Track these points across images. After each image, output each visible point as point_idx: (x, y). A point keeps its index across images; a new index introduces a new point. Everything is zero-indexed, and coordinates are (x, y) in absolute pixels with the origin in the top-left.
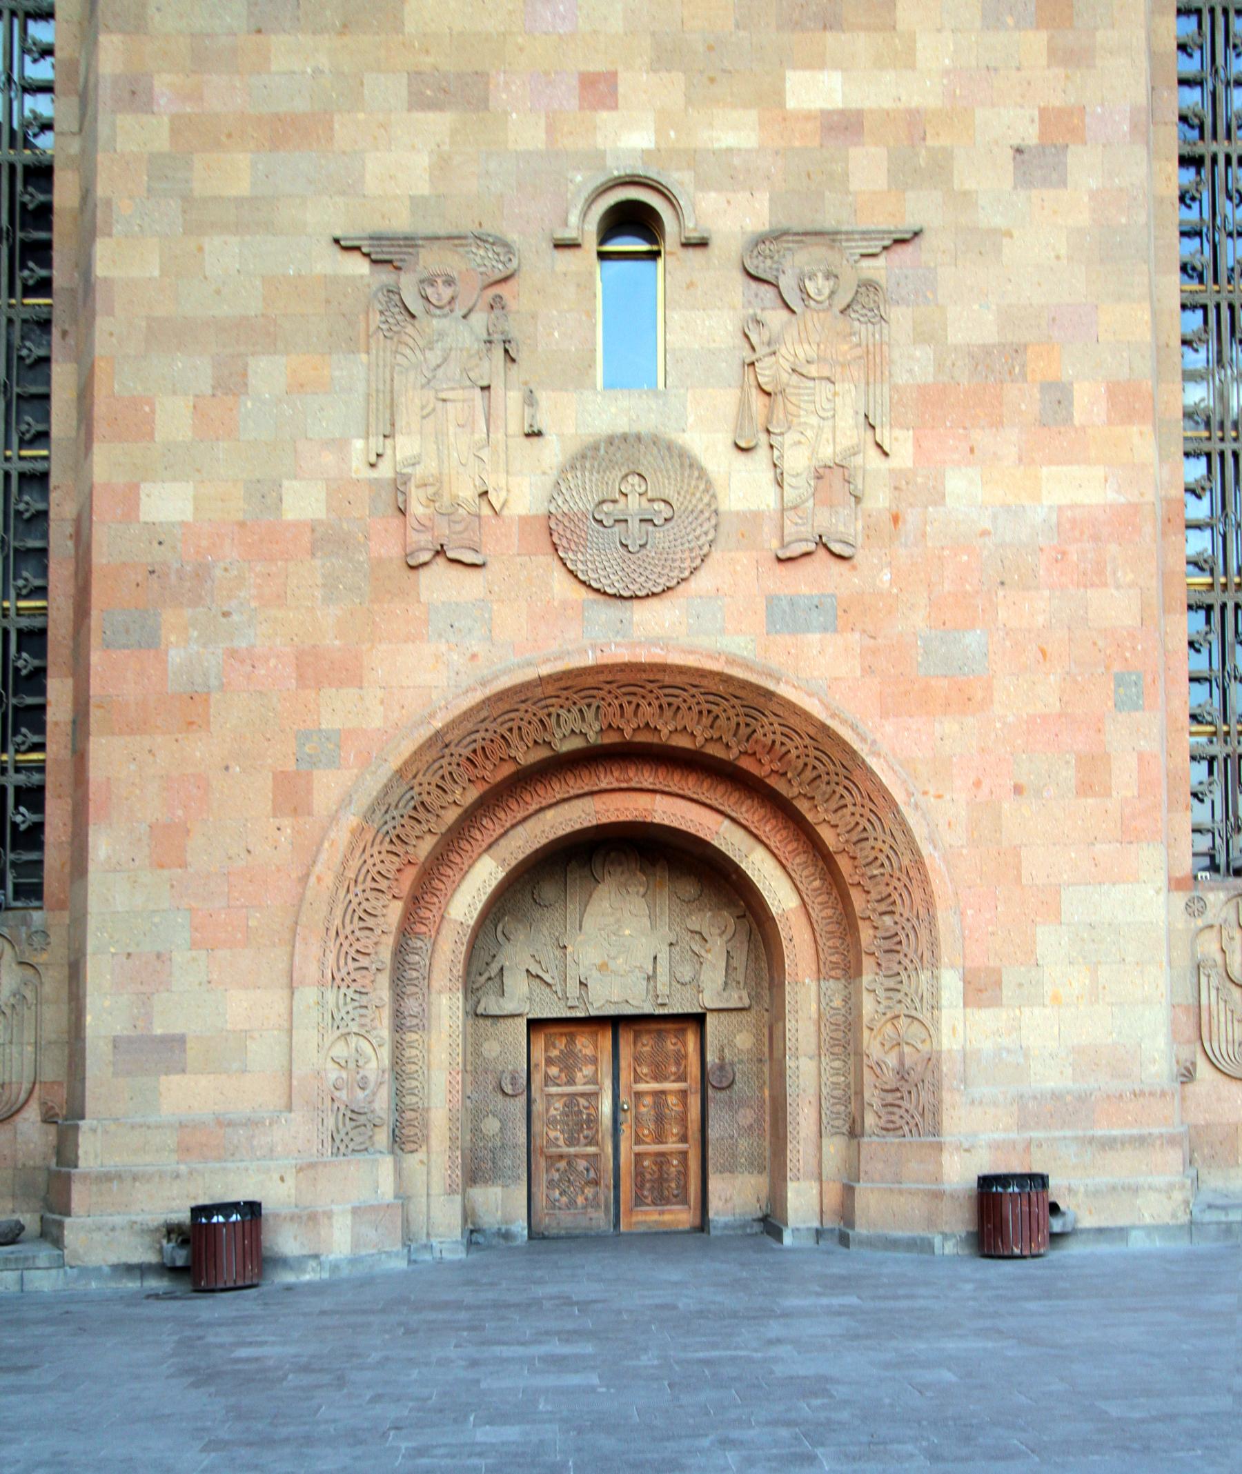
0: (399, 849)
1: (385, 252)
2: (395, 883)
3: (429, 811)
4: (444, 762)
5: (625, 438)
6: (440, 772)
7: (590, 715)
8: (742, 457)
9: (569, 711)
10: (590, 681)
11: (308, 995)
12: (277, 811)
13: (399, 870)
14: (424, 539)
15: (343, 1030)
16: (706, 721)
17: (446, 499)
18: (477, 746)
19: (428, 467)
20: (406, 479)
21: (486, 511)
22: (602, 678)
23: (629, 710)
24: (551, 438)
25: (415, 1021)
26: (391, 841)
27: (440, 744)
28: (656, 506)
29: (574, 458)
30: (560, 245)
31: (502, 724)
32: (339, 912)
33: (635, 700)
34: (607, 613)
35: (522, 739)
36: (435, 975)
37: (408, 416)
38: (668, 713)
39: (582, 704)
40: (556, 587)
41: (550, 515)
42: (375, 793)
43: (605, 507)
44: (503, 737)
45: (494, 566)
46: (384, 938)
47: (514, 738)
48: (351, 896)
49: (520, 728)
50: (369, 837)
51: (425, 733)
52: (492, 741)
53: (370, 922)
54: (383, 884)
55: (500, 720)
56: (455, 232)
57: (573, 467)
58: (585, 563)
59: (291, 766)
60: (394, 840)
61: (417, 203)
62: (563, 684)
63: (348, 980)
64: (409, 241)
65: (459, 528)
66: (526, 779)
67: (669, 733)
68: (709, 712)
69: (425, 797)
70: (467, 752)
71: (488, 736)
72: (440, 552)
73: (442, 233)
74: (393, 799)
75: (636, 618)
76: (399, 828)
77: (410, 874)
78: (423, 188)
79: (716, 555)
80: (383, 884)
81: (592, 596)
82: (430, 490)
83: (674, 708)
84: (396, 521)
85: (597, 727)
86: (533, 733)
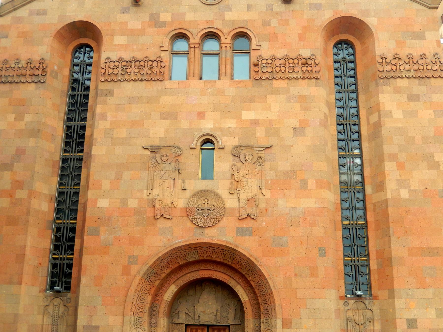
0: (151, 284)
1: (154, 149)
5: (204, 191)
7: (196, 253)
8: (231, 195)
10: (195, 246)
11: (127, 318)
12: (123, 274)
14: (159, 213)
15: (136, 327)
17: (164, 204)
19: (160, 197)
20: (155, 199)
21: (173, 206)
22: (198, 245)
23: (205, 253)
24: (188, 191)
25: (154, 325)
27: (160, 260)
28: (211, 206)
29: (193, 195)
30: (191, 148)
32: (136, 298)
33: (206, 250)
34: (199, 231)
36: (160, 313)
37: (156, 185)
38: (214, 254)
39: (194, 251)
40: (188, 224)
41: (187, 208)
43: (199, 206)
45: (174, 220)
46: (147, 305)
47: (178, 258)
48: (139, 295)
50: (143, 281)
51: (157, 257)
53: (143, 301)
54: (147, 292)
56: (169, 145)
57: (192, 197)
58: (194, 219)
59: (126, 264)
61: (161, 139)
62: (189, 247)
63: (137, 315)
64: (159, 147)
65: (167, 210)
66: (181, 267)
67: (214, 258)
69: (157, 272)
70: (167, 261)
72: (162, 216)
73: (166, 145)
74: (149, 272)
75: (206, 232)
77: (153, 290)
78: (162, 136)
79: (225, 218)
80: (147, 292)
81: (196, 226)
82: (161, 202)
84: (153, 208)
85: (198, 256)
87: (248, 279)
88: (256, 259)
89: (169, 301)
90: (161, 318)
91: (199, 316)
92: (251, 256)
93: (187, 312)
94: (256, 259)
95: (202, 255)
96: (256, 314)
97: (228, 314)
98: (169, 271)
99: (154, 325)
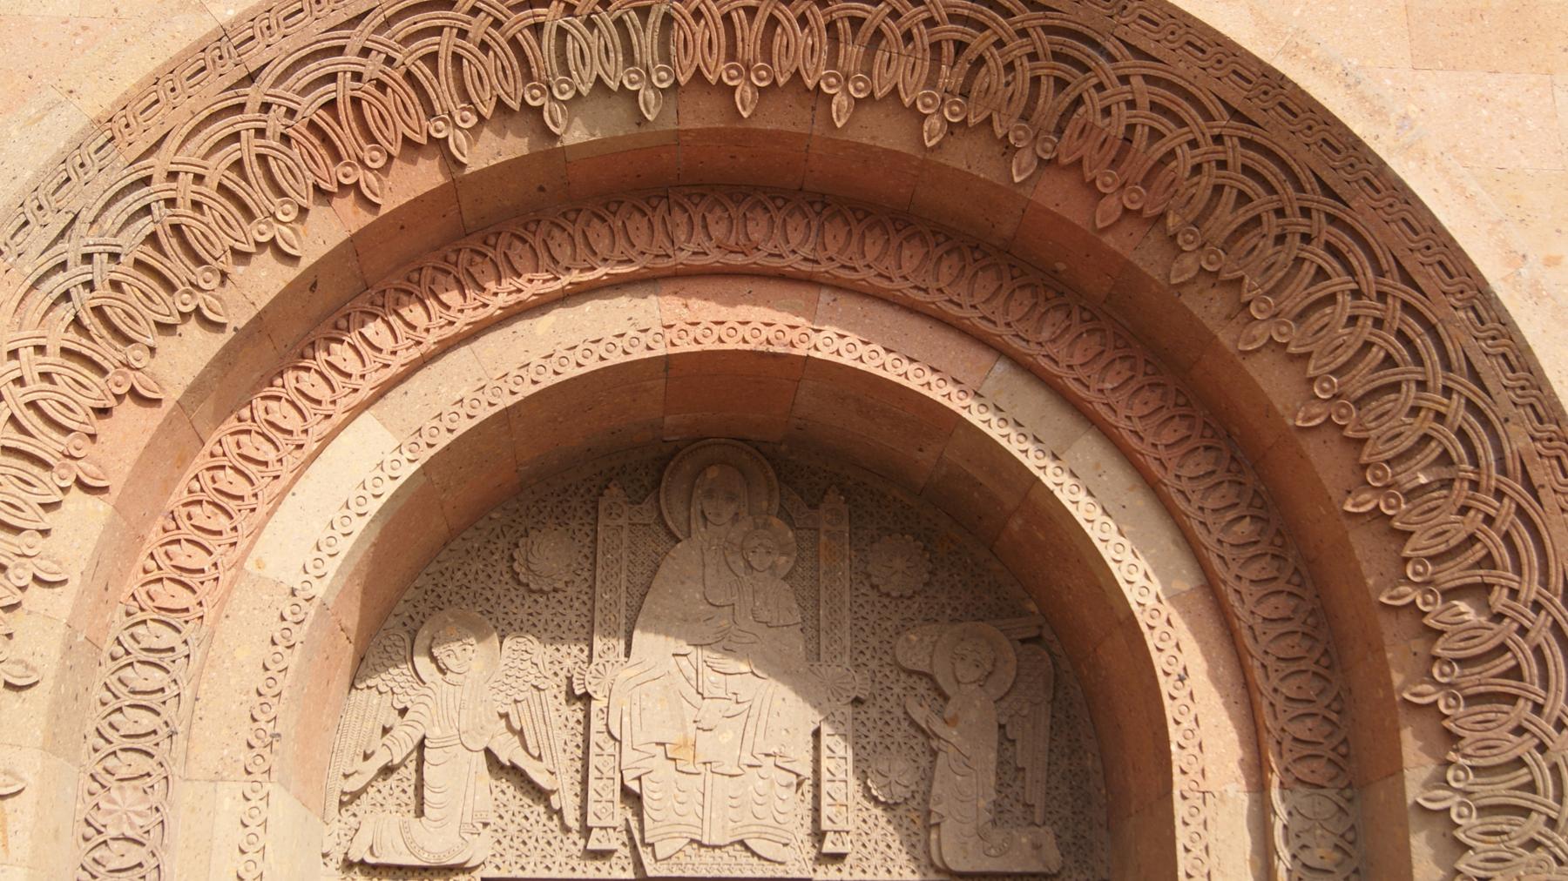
0: (105, 350)
2: (87, 448)
3: (199, 261)
4: (242, 123)
6: (231, 152)
7: (646, 42)
9: (590, 24)
13: (103, 412)
16: (949, 76)
18: (342, 90)
26: (77, 322)
31: (407, 40)
35: (464, 95)
38: (852, 52)
42: (28, 174)
44: (409, 75)
47: (443, 92)
49: (457, 59)
52: (381, 86)
55: (403, 27)
60: (88, 319)
68: (960, 46)
70: (308, 107)
71: (373, 67)
76: (103, 289)
83: (867, 31)
86: (494, 81)
87: (1225, 337)
88: (1348, 80)
89: (319, 589)
90: (218, 778)
91: (632, 798)
92: (1293, 51)
93: (509, 751)
94: (1348, 80)
95: (718, 70)
96: (1301, 730)
97: (928, 778)
98: (326, 231)
99: (134, 855)
